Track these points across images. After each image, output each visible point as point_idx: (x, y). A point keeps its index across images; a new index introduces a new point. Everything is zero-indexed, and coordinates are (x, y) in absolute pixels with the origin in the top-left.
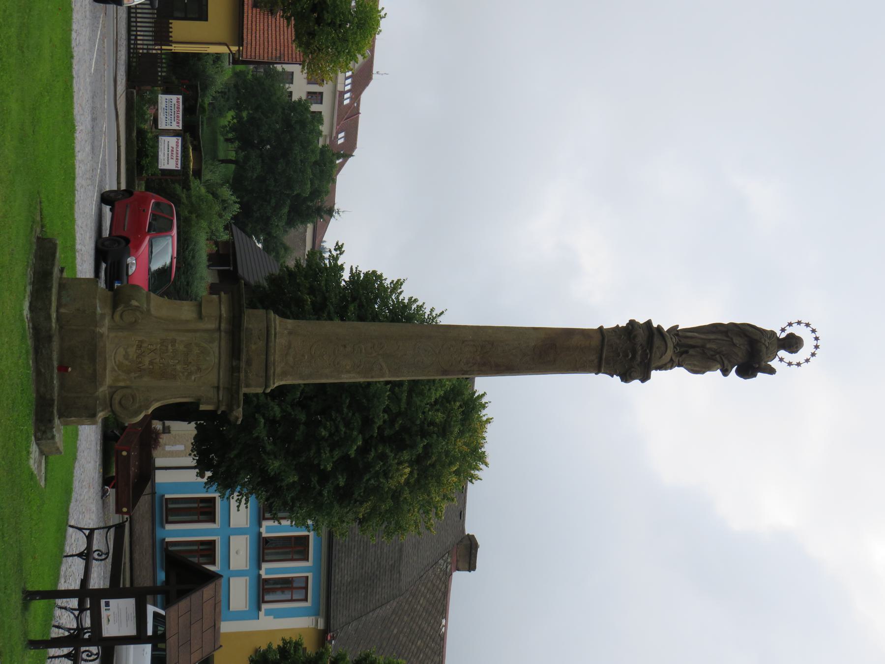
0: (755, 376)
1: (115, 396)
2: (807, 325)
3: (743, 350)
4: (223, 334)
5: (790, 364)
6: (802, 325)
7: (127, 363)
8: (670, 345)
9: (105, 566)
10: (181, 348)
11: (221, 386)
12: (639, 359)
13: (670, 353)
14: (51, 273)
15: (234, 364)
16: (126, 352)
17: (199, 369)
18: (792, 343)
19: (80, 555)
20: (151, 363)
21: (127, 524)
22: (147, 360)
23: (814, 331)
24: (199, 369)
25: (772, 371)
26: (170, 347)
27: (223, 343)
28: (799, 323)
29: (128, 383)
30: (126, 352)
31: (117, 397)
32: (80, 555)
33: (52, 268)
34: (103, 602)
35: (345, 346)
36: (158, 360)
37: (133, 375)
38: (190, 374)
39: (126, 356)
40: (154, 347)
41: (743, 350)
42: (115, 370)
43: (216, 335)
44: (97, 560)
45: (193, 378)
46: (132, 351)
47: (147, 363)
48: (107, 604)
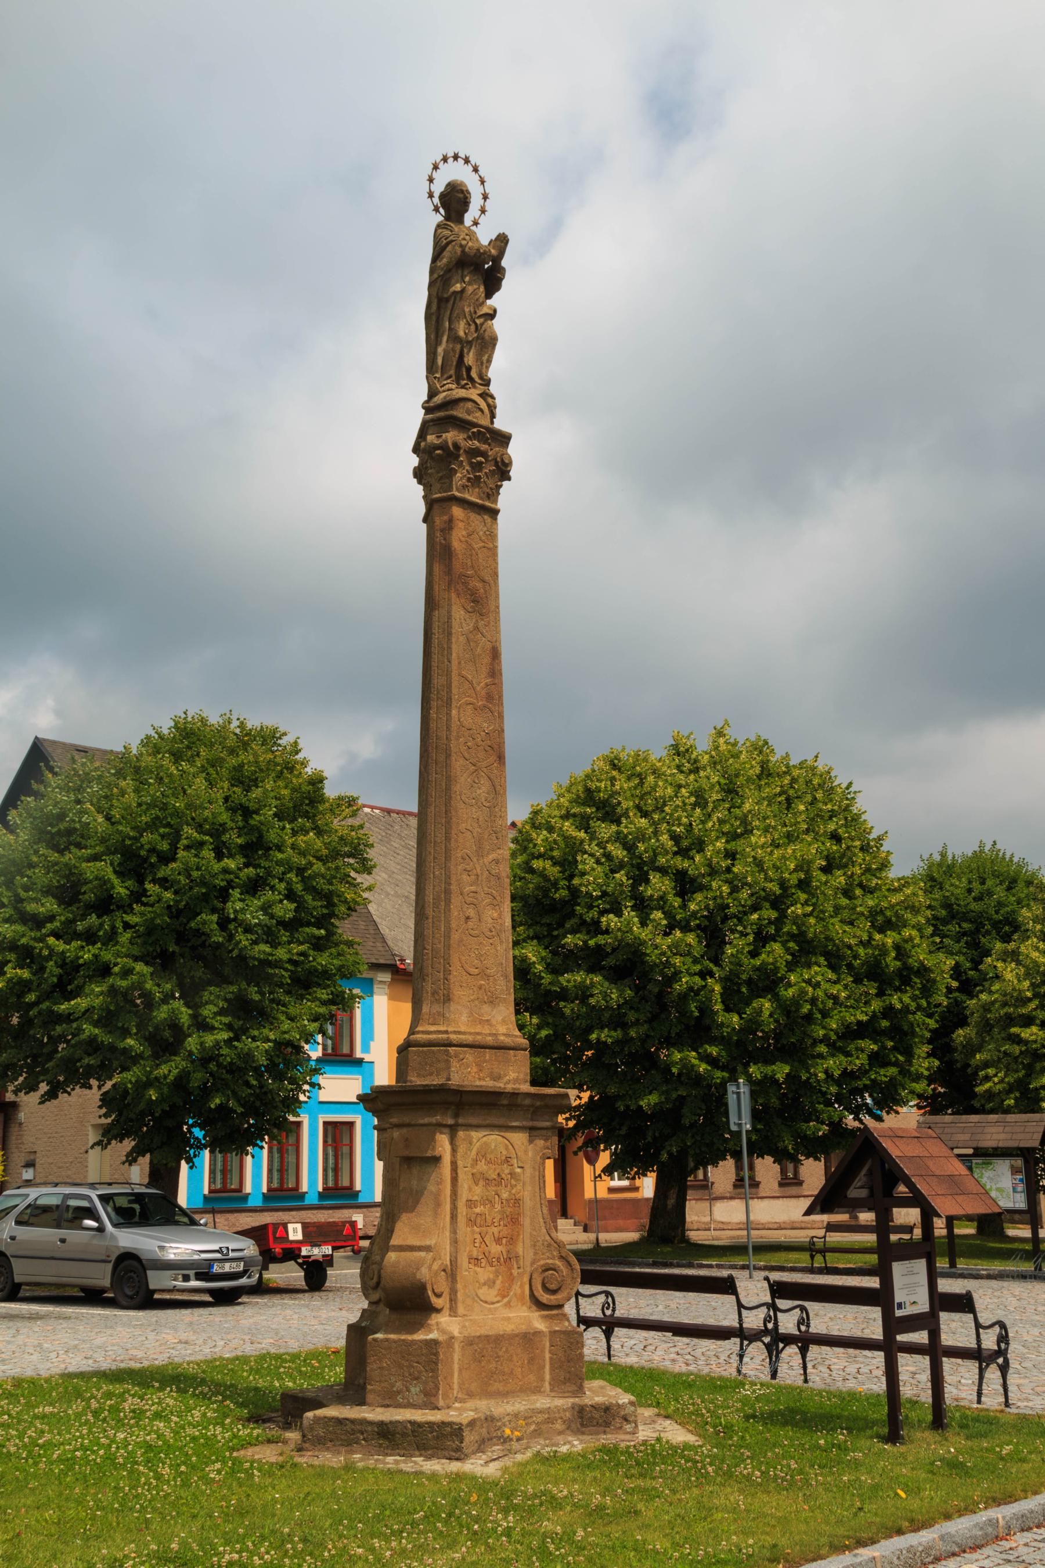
0: (504, 269)
1: (545, 1301)
2: (436, 167)
3: (465, 275)
4: (461, 1121)
5: (483, 211)
6: (435, 175)
7: (498, 1282)
8: (462, 393)
9: (620, 1295)
10: (478, 1190)
11: (530, 1124)
12: (484, 447)
13: (473, 394)
14: (381, 1424)
15: (505, 1102)
16: (484, 1284)
17: (507, 1160)
18: (454, 202)
19: (608, 1334)
20: (498, 1241)
21: (775, 1276)
22: (496, 1249)
23: (445, 159)
24: (507, 1160)
25: (502, 241)
26: (478, 1210)
27: (474, 1121)
28: (431, 180)
29: (526, 1279)
30: (484, 1284)
31: (545, 1298)
32: (608, 1334)
33: (371, 1423)
34: (899, 1313)
35: (468, 918)
36: (495, 1230)
37: (515, 1272)
38: (512, 1174)
39: (490, 1283)
40: (478, 1236)
41: (465, 275)
42: (509, 1302)
43: (461, 1134)
44: (614, 1310)
45: (518, 1170)
46: (484, 1273)
47: (499, 1248)
48: (900, 1306)
